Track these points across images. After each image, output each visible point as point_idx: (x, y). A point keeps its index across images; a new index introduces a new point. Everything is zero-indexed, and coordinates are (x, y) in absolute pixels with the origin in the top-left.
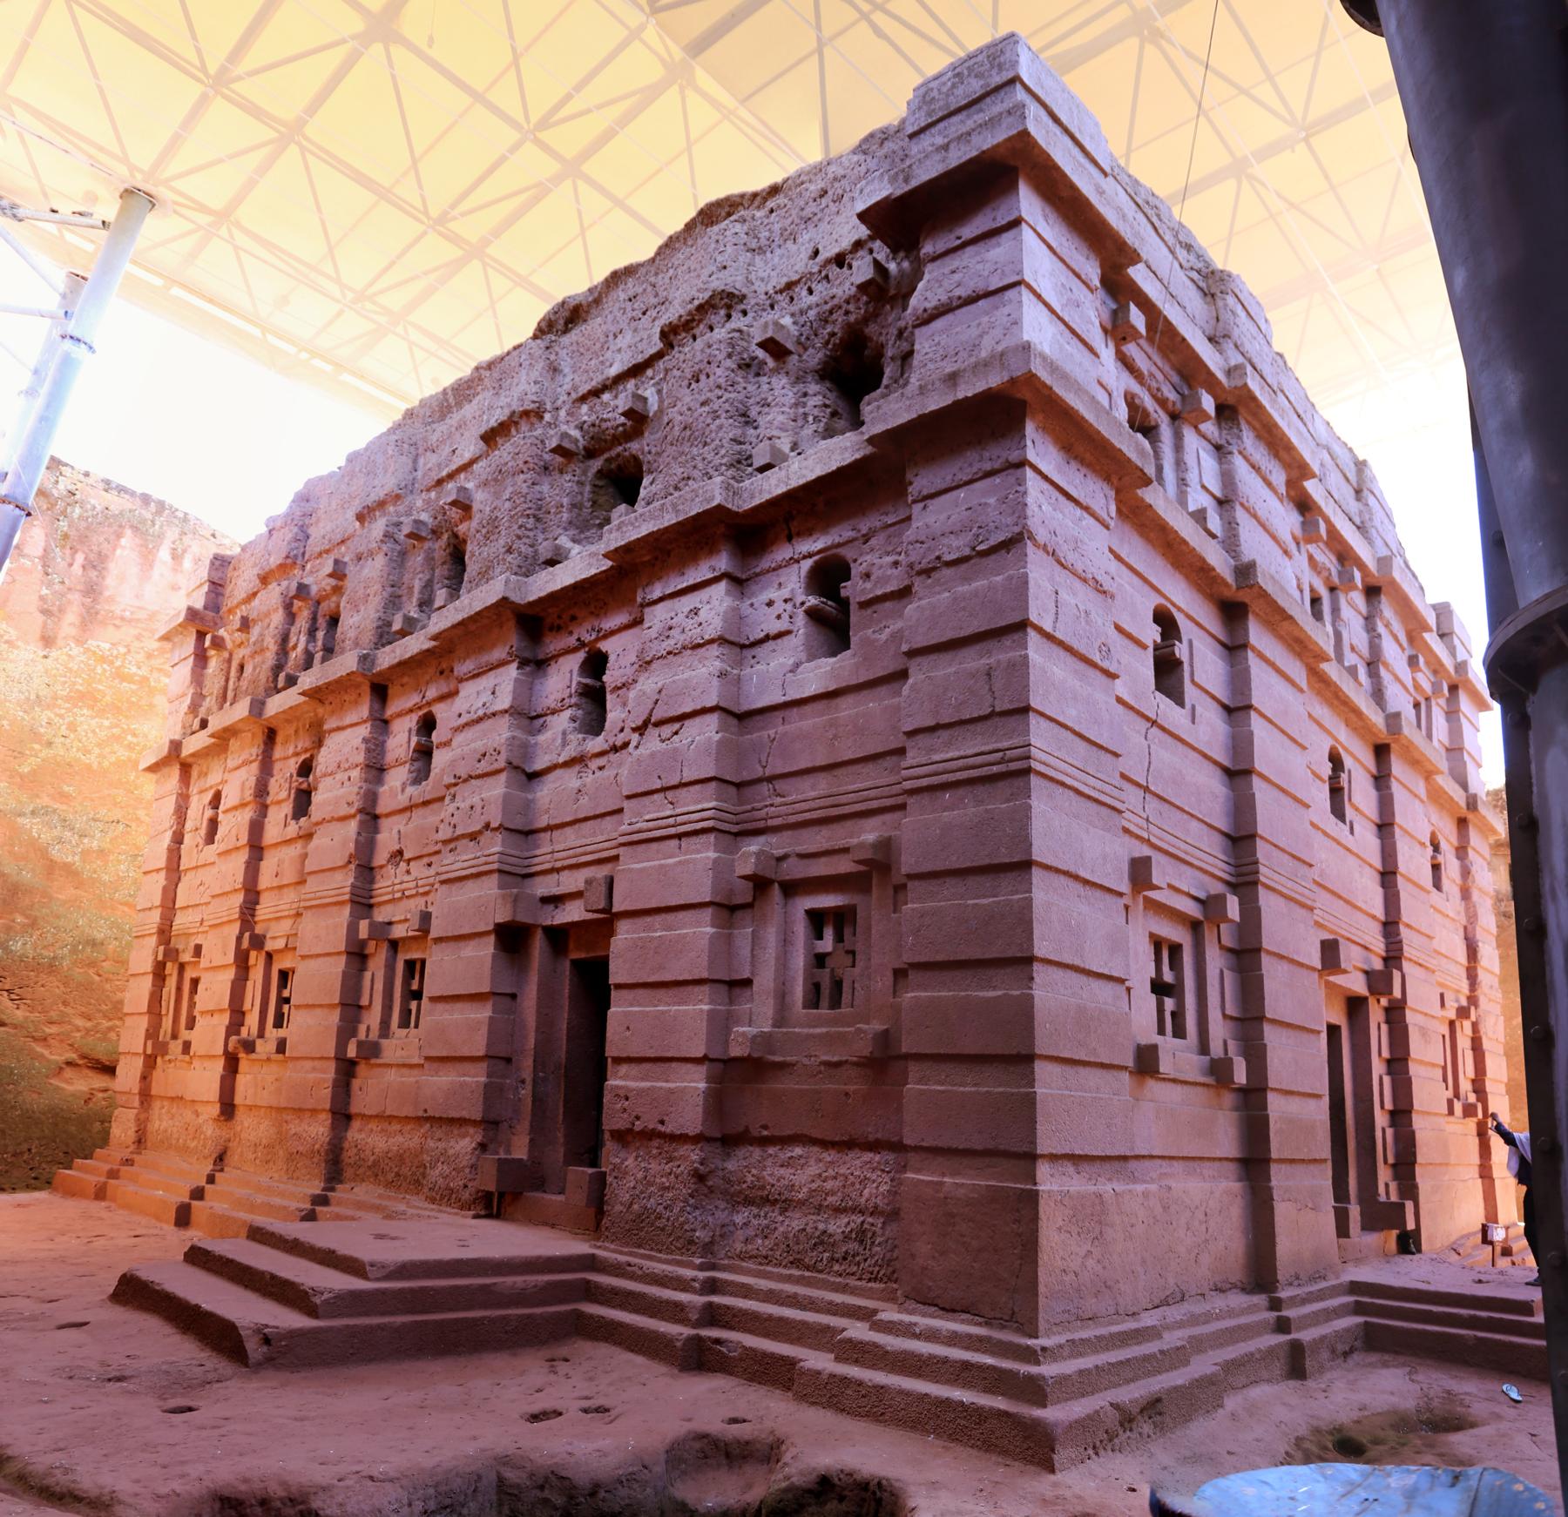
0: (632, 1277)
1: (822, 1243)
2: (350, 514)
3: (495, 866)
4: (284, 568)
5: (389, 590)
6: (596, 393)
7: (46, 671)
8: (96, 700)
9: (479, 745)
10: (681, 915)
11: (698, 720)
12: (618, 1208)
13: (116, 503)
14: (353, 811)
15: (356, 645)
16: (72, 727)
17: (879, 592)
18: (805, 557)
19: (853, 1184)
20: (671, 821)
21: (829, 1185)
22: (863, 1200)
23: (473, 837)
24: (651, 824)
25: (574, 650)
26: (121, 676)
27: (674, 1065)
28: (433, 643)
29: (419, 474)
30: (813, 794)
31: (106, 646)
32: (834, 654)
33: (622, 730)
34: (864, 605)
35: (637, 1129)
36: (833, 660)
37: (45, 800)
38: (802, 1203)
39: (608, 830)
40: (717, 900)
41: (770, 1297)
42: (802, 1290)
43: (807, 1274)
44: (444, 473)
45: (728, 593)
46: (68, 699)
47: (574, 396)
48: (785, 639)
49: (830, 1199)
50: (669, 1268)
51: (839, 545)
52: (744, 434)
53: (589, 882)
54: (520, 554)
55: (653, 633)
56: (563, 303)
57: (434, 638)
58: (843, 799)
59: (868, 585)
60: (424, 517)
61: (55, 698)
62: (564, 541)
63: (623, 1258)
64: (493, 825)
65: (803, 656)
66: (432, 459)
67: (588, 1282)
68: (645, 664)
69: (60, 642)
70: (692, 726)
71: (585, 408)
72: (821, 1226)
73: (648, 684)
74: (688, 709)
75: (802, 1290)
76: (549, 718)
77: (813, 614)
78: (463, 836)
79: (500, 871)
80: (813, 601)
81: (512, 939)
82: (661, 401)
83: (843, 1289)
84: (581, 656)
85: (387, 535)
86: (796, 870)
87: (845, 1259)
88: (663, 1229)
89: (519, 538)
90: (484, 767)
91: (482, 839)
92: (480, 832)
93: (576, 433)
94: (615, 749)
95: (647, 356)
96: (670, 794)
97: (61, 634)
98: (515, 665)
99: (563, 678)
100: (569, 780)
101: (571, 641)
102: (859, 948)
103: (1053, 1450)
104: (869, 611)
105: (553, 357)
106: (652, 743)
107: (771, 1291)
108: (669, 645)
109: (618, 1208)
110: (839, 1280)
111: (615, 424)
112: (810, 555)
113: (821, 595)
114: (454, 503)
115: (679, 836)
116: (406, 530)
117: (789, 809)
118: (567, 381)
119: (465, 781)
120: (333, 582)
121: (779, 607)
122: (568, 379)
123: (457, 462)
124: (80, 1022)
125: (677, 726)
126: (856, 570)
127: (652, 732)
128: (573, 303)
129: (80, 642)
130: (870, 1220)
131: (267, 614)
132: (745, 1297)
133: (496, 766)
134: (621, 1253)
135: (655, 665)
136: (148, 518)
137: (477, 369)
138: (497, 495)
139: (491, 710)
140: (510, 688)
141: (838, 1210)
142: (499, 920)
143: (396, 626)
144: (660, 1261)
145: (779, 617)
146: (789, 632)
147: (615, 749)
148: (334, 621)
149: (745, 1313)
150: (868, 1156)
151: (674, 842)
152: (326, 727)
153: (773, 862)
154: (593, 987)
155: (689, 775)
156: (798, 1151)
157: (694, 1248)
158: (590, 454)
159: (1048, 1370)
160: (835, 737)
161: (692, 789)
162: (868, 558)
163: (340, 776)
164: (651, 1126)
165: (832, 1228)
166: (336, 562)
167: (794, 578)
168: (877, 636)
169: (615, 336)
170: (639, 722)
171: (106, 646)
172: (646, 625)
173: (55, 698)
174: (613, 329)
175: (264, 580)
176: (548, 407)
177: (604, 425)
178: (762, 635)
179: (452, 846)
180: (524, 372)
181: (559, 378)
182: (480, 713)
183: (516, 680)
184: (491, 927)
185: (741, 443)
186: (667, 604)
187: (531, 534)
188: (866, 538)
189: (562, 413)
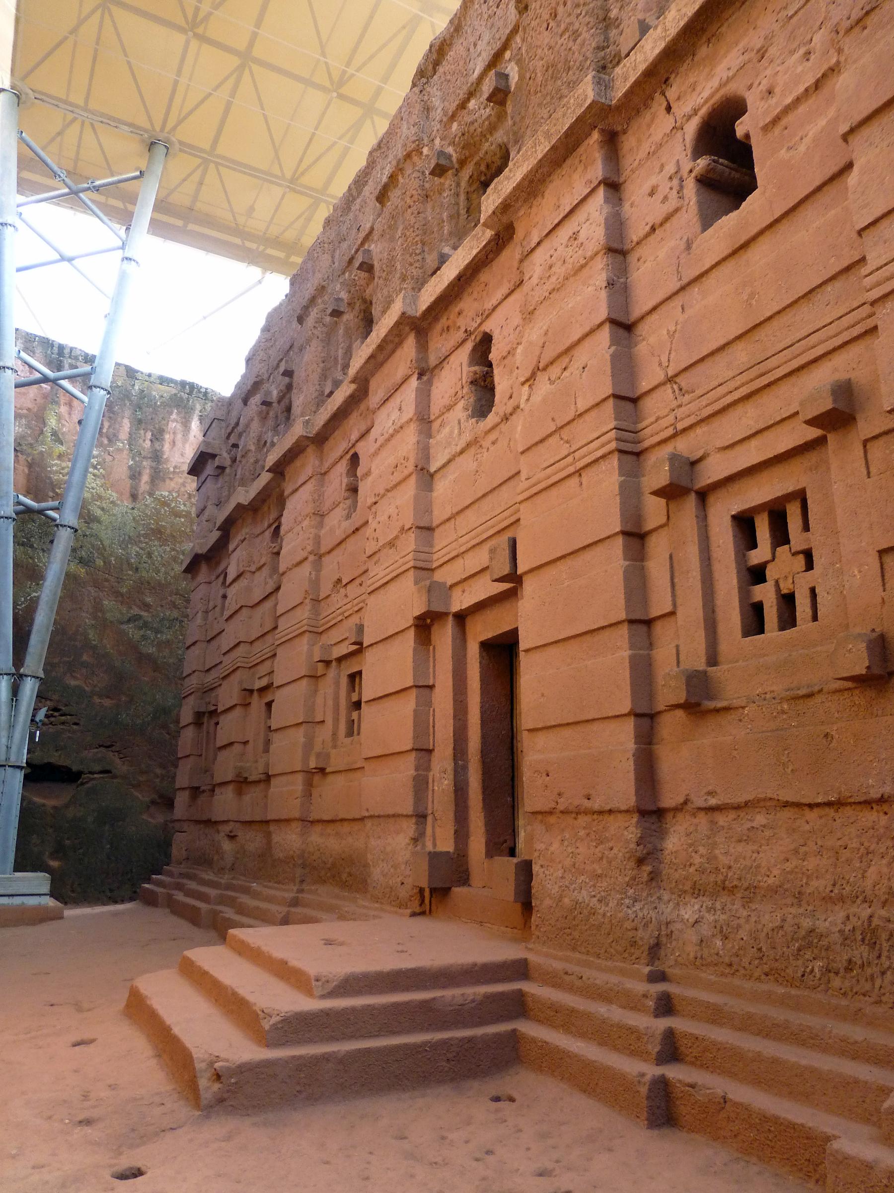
0: (571, 989)
1: (810, 945)
2: (295, 324)
3: (411, 564)
4: (256, 386)
5: (322, 365)
6: (463, 105)
7: (134, 519)
8: (160, 532)
9: (391, 460)
10: (588, 555)
11: (587, 343)
12: (548, 902)
13: (167, 391)
14: (304, 554)
15: (302, 415)
16: (149, 555)
17: (789, 100)
18: (689, 117)
19: (849, 861)
20: (570, 459)
21: (811, 863)
22: (869, 883)
23: (391, 544)
24: (549, 470)
25: (464, 341)
26: (177, 514)
27: (595, 727)
28: (353, 386)
29: (336, 264)
30: (731, 374)
31: (167, 494)
32: (737, 207)
33: (511, 397)
34: (766, 129)
35: (561, 807)
36: (734, 215)
37: (135, 611)
38: (774, 890)
39: (507, 496)
40: (628, 528)
43: (794, 992)
44: (353, 252)
45: (607, 200)
46: (146, 536)
47: (445, 119)
48: (674, 220)
49: (814, 883)
50: (614, 979)
51: (729, 80)
52: (607, 39)
53: (492, 551)
54: (412, 278)
55: (535, 280)
56: (431, 47)
57: (353, 381)
58: (773, 362)
59: (773, 101)
60: (344, 295)
61: (139, 536)
62: (447, 250)
63: (558, 965)
64: (406, 527)
65: (698, 227)
66: (345, 245)
67: (521, 994)
68: (529, 315)
69: (140, 497)
70: (582, 356)
71: (455, 126)
72: (806, 923)
73: (534, 334)
74: (576, 337)
76: (446, 415)
77: (706, 182)
78: (384, 546)
79: (415, 567)
80: (703, 162)
81: (425, 625)
82: (521, 77)
83: (856, 1017)
84: (469, 346)
85: (319, 321)
86: (716, 469)
87: (848, 969)
88: (599, 927)
89: (411, 264)
90: (398, 477)
91: (398, 543)
92: (396, 537)
93: (450, 150)
94: (506, 418)
95: (504, 38)
96: (565, 433)
97: (141, 491)
98: (416, 376)
99: (456, 373)
100: (467, 463)
101: (461, 335)
102: (816, 539)
104: (777, 130)
105: (426, 98)
106: (543, 387)
107: (750, 1016)
108: (549, 286)
109: (548, 902)
111: (480, 121)
112: (695, 112)
113: (711, 154)
114: (360, 268)
115: (579, 472)
116: (329, 311)
117: (704, 401)
118: (437, 114)
119: (384, 495)
120: (287, 380)
121: (663, 190)
122: (439, 110)
123: (362, 235)
124: (159, 771)
125: (565, 360)
126: (752, 99)
127: (542, 378)
128: (438, 42)
129: (151, 494)
130: (883, 913)
131: (247, 426)
132: (714, 1022)
133: (406, 472)
134: (555, 958)
135: (537, 312)
136: (186, 395)
137: (370, 153)
138: (392, 239)
139: (399, 425)
140: (413, 396)
141: (829, 900)
142: (417, 613)
143: (327, 391)
145: (666, 198)
146: (677, 210)
147: (506, 418)
148: (288, 409)
150: (869, 817)
151: (575, 480)
152: (286, 493)
153: (687, 468)
154: (503, 653)
155: (582, 406)
156: (760, 819)
157: (637, 953)
158: (462, 163)
160: (752, 296)
161: (587, 417)
162: (768, 72)
163: (298, 529)
164: (576, 803)
165: (822, 926)
166: (287, 362)
167: (679, 148)
168: (792, 152)
169: (475, 45)
170: (528, 374)
171: (167, 494)
172: (526, 278)
173: (139, 536)
174: (472, 40)
175: (245, 402)
176: (426, 141)
177: (472, 129)
178: (648, 228)
179: (376, 558)
180: (405, 123)
181: (432, 114)
182: (391, 431)
183: (417, 389)
184: (411, 622)
185: (603, 48)
186: (545, 245)
187: (420, 258)
188: (762, 54)
189: (437, 141)
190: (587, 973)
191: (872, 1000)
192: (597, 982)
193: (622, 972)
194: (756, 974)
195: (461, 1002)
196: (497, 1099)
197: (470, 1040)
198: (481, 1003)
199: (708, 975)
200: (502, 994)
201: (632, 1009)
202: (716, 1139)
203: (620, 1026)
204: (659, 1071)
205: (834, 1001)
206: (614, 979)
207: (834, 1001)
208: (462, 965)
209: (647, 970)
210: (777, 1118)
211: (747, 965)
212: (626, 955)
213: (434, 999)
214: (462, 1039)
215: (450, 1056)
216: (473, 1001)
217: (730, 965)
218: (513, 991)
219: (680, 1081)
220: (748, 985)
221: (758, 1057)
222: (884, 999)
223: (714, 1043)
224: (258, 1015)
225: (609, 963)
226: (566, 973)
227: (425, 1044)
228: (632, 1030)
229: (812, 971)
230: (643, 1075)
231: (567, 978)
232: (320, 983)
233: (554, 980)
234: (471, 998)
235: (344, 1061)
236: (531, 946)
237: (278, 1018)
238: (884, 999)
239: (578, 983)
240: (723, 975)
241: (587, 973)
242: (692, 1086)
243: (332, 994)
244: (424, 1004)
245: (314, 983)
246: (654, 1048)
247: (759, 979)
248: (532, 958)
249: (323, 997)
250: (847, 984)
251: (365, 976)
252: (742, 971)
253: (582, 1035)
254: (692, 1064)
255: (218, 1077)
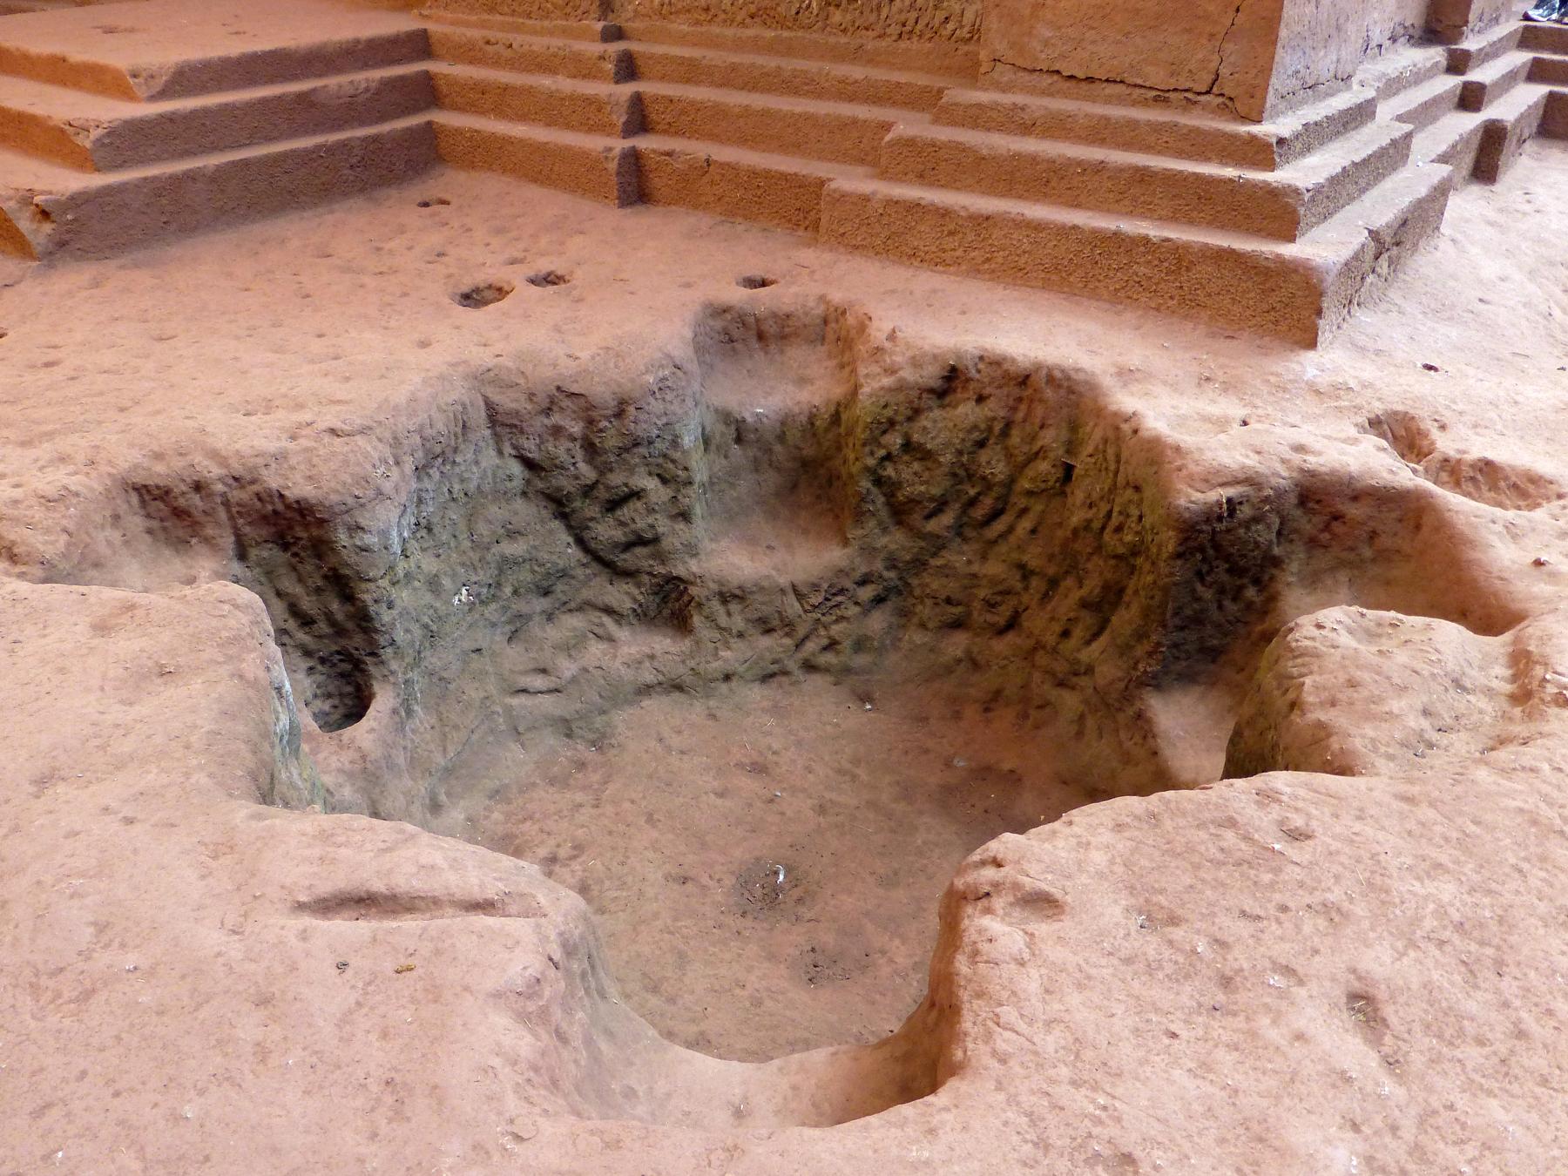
41: (730, 78)
42: (791, 64)
43: (786, 34)
50: (556, 42)
63: (475, 34)
67: (428, 77)
75: (770, 62)
83: (856, 55)
103: (1319, 312)
107: (734, 68)
110: (843, 40)
134: (467, 24)
144: (535, 33)
149: (697, 106)
159: (1287, 175)
190: (518, 39)
191: (875, 34)
192: (535, 48)
193: (565, 32)
194: (739, 19)
195: (352, 92)
196: (426, 205)
197: (375, 139)
198: (378, 92)
199: (681, 26)
200: (402, 78)
201: (584, 77)
202: (696, 207)
203: (572, 98)
204: (628, 143)
205: (832, 40)
206: (556, 42)
207: (832, 40)
208: (341, 43)
209: (600, 25)
210: (768, 171)
211: (728, 7)
212: (568, 10)
213: (314, 90)
214: (364, 139)
215: (354, 161)
216: (367, 90)
217: (707, 9)
218: (418, 73)
219: (654, 151)
220: (730, 32)
221: (747, 112)
222: (888, 31)
223: (692, 103)
224: (62, 131)
225: (546, 23)
226: (488, 43)
227: (318, 147)
228: (589, 101)
229: (809, 6)
230: (610, 149)
231: (489, 48)
232: (141, 80)
233: (469, 53)
234: (364, 85)
235: (217, 178)
236: (425, 12)
237: (100, 131)
238: (888, 31)
239: (508, 53)
240: (698, 23)
241: (518, 39)
242: (669, 154)
243: (164, 94)
244: (301, 97)
245: (131, 81)
246: (620, 119)
247: (742, 24)
248: (431, 26)
249: (153, 98)
250: (849, 17)
251: (206, 65)
252: (723, 16)
253: (522, 117)
254: (665, 132)
255: (45, 214)
